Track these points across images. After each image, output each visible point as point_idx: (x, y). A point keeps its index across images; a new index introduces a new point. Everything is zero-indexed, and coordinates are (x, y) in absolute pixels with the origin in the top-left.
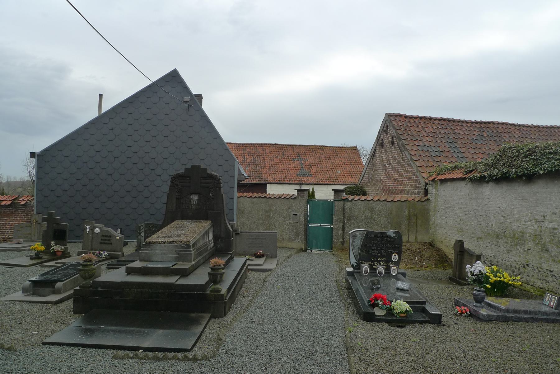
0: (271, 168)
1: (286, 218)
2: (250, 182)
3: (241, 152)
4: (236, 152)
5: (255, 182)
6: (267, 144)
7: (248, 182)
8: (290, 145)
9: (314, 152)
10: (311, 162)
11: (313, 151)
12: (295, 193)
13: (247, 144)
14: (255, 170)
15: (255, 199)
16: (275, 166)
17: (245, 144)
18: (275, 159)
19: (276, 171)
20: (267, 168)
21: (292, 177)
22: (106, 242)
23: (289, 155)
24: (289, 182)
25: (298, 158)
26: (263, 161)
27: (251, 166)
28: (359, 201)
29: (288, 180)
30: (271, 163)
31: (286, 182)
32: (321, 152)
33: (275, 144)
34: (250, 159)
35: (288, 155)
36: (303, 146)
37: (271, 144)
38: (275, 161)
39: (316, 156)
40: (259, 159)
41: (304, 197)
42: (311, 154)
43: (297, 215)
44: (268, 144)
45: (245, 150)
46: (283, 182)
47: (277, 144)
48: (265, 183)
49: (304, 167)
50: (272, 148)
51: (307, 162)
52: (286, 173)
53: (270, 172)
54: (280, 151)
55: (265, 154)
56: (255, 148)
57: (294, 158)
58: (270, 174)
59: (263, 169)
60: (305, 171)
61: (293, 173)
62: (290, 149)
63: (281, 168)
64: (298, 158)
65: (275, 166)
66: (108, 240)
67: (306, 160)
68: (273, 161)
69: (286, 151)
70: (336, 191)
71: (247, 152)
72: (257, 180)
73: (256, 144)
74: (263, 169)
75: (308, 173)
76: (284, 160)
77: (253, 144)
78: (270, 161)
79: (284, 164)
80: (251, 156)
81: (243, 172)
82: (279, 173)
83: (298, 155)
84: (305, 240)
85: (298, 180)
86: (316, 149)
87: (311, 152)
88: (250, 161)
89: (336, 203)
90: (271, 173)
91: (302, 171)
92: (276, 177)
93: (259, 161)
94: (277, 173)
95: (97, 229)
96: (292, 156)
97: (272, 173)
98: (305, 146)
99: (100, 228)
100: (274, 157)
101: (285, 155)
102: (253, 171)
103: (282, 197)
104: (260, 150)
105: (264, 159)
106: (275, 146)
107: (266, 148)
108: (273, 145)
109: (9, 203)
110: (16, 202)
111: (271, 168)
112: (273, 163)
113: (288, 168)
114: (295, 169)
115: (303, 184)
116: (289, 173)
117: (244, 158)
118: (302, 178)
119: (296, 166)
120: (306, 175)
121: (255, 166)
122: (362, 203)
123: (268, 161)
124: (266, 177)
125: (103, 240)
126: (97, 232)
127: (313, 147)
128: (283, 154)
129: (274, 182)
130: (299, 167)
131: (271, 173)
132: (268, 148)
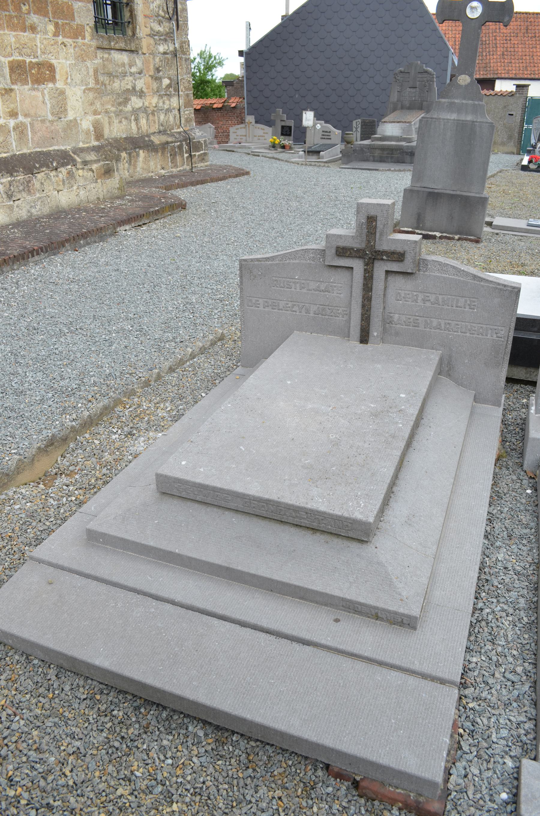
0: (505, 53)
1: (501, 118)
4: (454, 29)
12: (514, 89)
16: (512, 50)
18: (512, 38)
19: (513, 57)
20: (499, 53)
21: (536, 69)
22: (326, 137)
24: (529, 77)
26: (494, 42)
29: (529, 72)
30: (505, 45)
31: (526, 76)
35: (534, 32)
38: (513, 42)
41: (522, 94)
43: (512, 115)
46: (521, 76)
48: (493, 78)
52: (528, 61)
54: (522, 24)
55: (498, 31)
58: (503, 64)
63: (520, 54)
65: (512, 50)
66: (328, 135)
68: (509, 42)
69: (533, 24)
72: (481, 73)
74: (493, 55)
78: (505, 42)
79: (527, 46)
82: (517, 61)
84: (518, 144)
90: (504, 62)
92: (510, 68)
93: (488, 42)
94: (513, 61)
95: (318, 125)
97: (506, 61)
99: (320, 124)
100: (512, 35)
101: (529, 31)
103: (499, 94)
105: (496, 39)
109: (220, 106)
110: (226, 104)
111: (505, 53)
112: (509, 45)
113: (531, 53)
116: (531, 61)
123: (502, 42)
125: (324, 135)
126: (318, 128)
128: (527, 30)
129: (507, 76)
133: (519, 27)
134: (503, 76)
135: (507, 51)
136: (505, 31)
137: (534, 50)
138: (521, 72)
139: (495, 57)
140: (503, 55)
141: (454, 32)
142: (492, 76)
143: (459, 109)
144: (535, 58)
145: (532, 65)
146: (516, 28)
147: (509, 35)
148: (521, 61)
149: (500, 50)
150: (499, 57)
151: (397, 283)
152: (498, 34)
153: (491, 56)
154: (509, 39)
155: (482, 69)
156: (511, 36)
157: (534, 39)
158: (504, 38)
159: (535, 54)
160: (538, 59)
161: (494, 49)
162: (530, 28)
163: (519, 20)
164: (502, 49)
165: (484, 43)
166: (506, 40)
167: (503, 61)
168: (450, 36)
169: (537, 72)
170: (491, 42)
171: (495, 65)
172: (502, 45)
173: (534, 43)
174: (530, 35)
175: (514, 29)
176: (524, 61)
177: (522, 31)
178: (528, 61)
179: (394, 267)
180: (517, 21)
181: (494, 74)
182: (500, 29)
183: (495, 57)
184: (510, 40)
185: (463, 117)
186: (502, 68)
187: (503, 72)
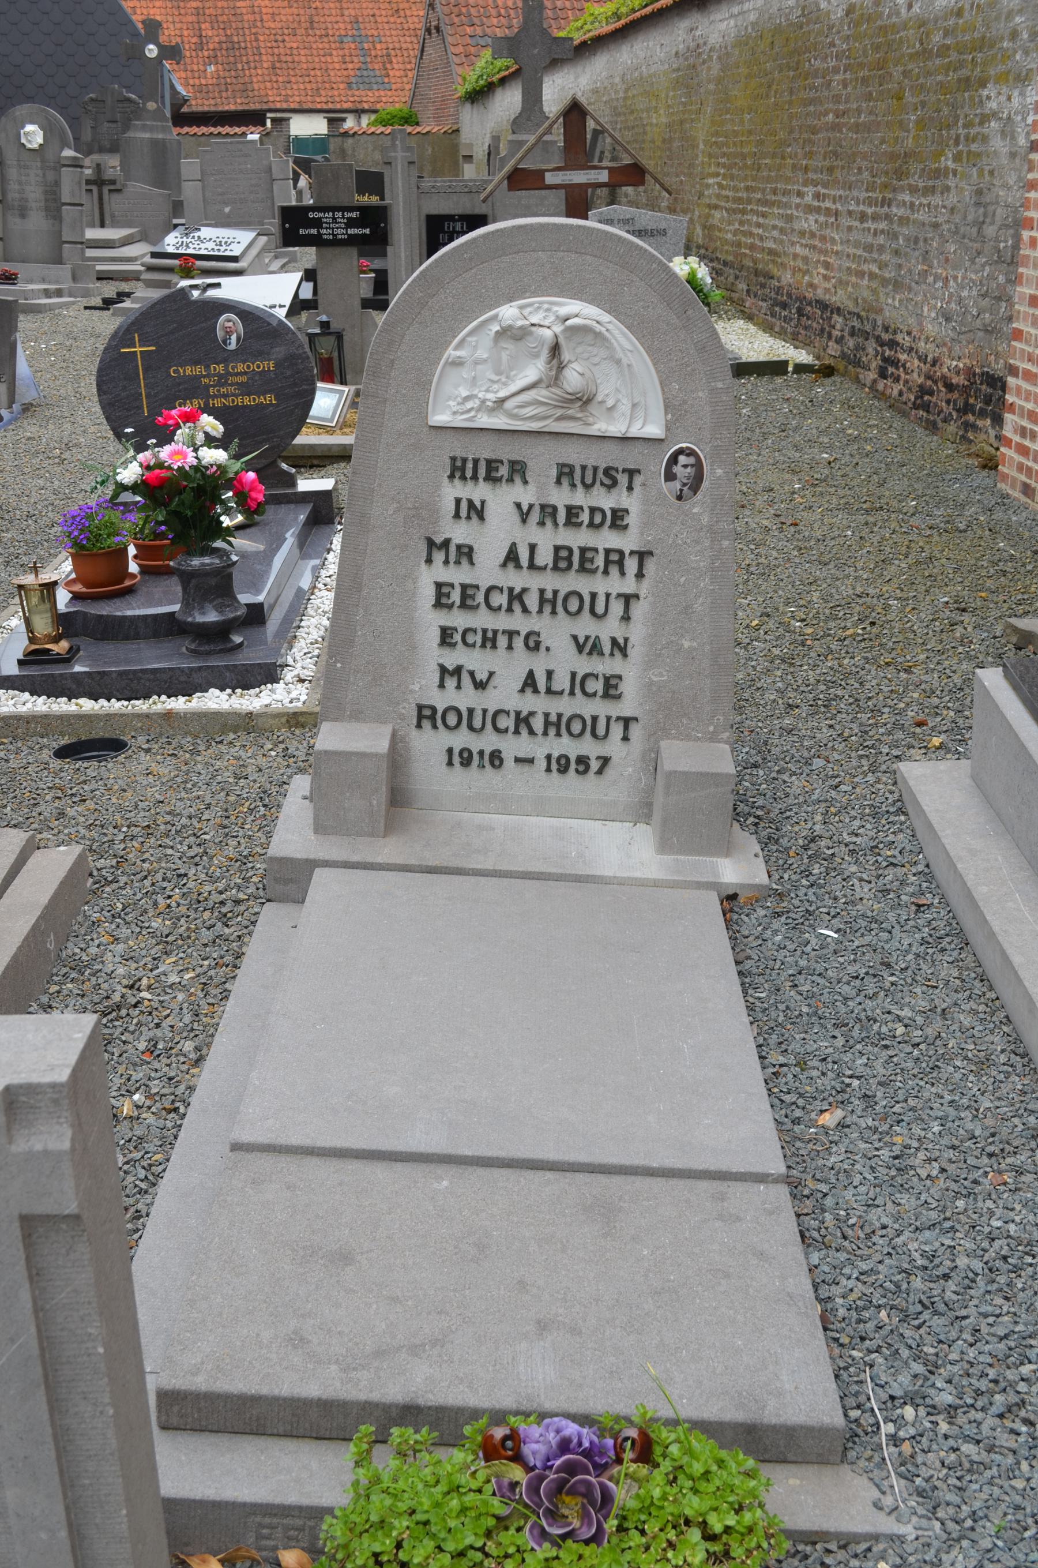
0: (278, 65)
2: (220, 109)
3: (190, 19)
4: (177, 19)
5: (232, 108)
7: (213, 109)
9: (402, 13)
10: (391, 46)
11: (397, 11)
14: (233, 73)
15: (203, 139)
16: (289, 59)
18: (286, 38)
19: (292, 73)
21: (336, 93)
23: (330, 26)
24: (325, 107)
25: (355, 32)
26: (254, 44)
27: (220, 59)
28: (365, 136)
29: (324, 99)
30: (276, 51)
31: (319, 106)
34: (217, 39)
35: (324, 26)
39: (406, 26)
40: (241, 39)
42: (392, 20)
45: (201, 12)
46: (311, 106)
48: (261, 110)
51: (378, 46)
52: (319, 79)
54: (302, 12)
55: (259, 24)
57: (343, 33)
59: (255, 68)
60: (372, 73)
61: (339, 79)
63: (305, 66)
64: (355, 32)
65: (289, 59)
67: (377, 39)
68: (281, 45)
69: (321, 12)
70: (330, 121)
71: (208, 19)
74: (255, 68)
75: (379, 80)
76: (312, 39)
78: (274, 44)
79: (315, 52)
80: (221, 32)
81: (180, 88)
82: (300, 80)
83: (355, 26)
85: (352, 99)
88: (217, 46)
89: (331, 139)
90: (277, 82)
91: (365, 73)
92: (290, 92)
93: (243, 45)
94: (293, 79)
96: (336, 26)
97: (281, 79)
100: (286, 31)
101: (315, 25)
102: (227, 74)
104: (244, 11)
105: (257, 40)
111: (278, 65)
112: (282, 51)
113: (323, 65)
114: (344, 66)
115: (364, 111)
116: (326, 79)
117: (201, 36)
118: (363, 93)
119: (348, 59)
120: (375, 87)
121: (232, 59)
122: (369, 138)
123: (269, 45)
124: (263, 93)
130: (356, 60)
131: (277, 82)
133: (297, 19)
134: (278, 106)
136: (272, 25)
137: (329, 59)
138: (309, 98)
141: (178, 26)
142: (257, 107)
143: (151, 129)
144: (332, 73)
145: (327, 86)
146: (291, 18)
148: (307, 79)
149: (267, 61)
151: (115, 196)
152: (260, 31)
153: (253, 71)
154: (280, 38)
155: (238, 94)
156: (283, 34)
157: (325, 40)
159: (331, 67)
160: (336, 75)
161: (257, 58)
162: (316, 19)
164: (271, 58)
165: (236, 46)
166: (276, 41)
167: (274, 79)
168: (173, 33)
169: (337, 99)
170: (249, 45)
171: (262, 87)
172: (270, 51)
173: (327, 46)
174: (318, 32)
175: (288, 20)
176: (312, 79)
177: (304, 25)
178: (319, 79)
179: (112, 187)
180: (291, 7)
183: (260, 72)
184: (284, 41)
185: (155, 136)
186: (275, 91)
187: (278, 99)
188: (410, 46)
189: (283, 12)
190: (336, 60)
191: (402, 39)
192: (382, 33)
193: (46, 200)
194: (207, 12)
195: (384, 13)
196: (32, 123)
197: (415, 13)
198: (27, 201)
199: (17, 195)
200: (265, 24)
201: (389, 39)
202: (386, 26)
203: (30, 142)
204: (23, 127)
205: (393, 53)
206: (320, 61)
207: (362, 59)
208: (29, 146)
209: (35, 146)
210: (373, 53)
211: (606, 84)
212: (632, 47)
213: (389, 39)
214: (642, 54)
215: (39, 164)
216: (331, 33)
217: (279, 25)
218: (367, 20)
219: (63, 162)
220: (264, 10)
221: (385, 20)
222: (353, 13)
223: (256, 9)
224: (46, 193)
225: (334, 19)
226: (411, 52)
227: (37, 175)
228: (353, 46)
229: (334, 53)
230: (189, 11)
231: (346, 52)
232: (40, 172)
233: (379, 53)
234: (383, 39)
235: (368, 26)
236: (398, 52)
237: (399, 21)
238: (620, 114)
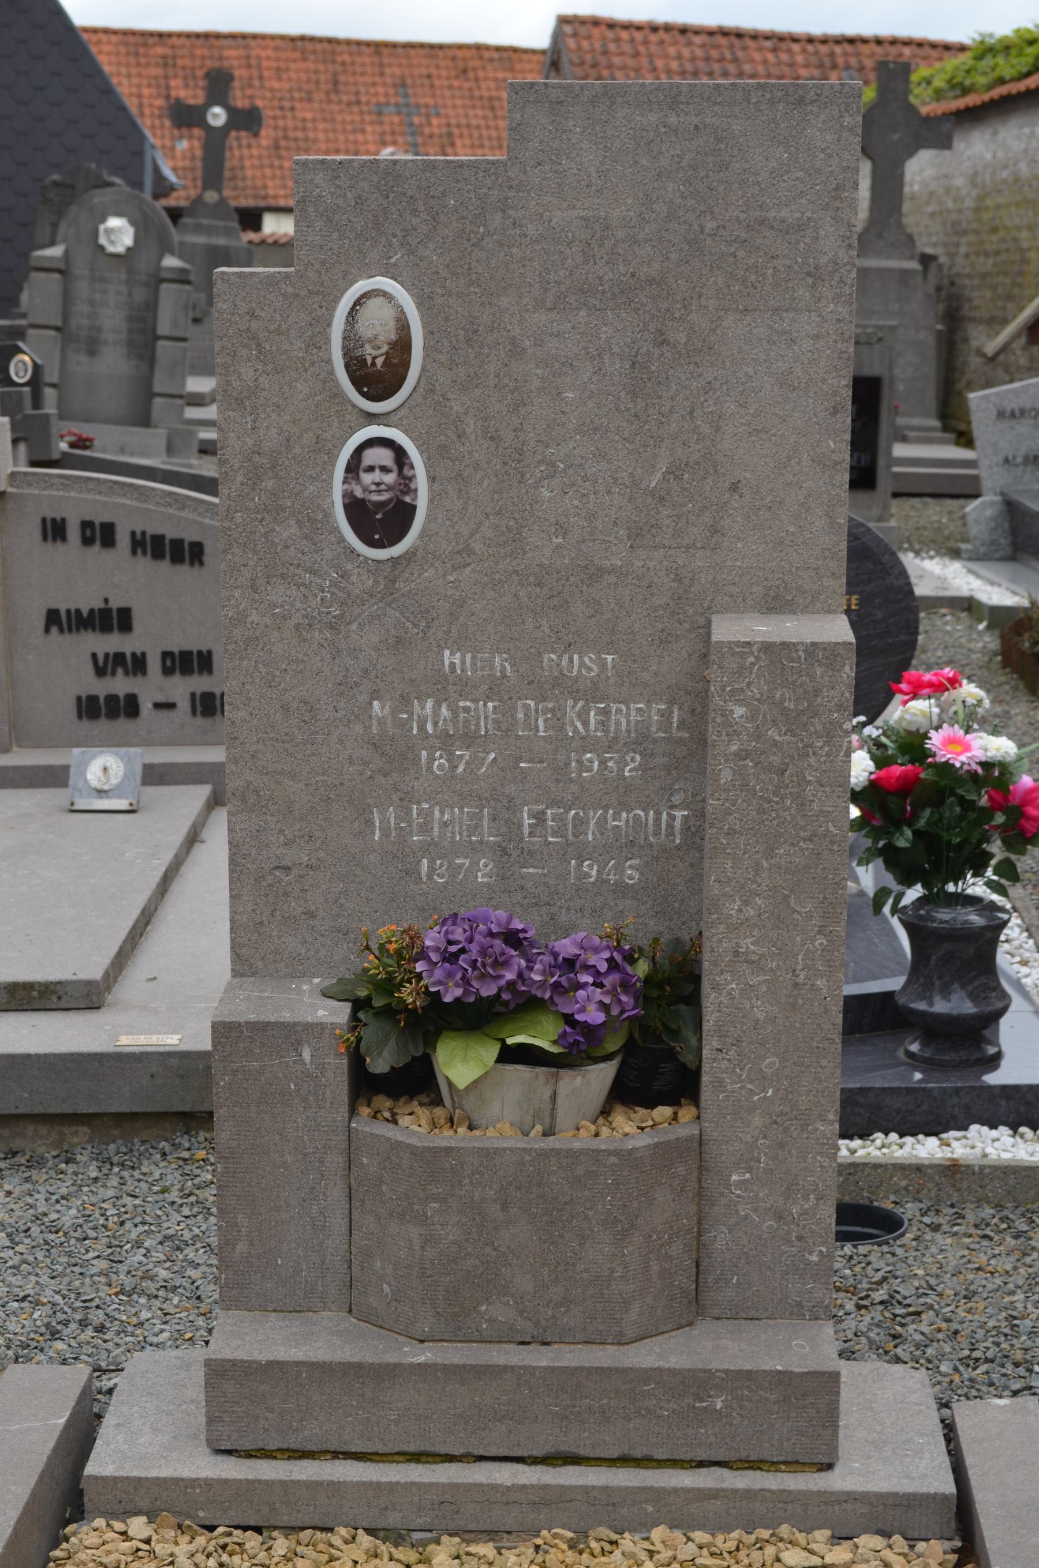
0: (283, 143)
3: (153, 71)
4: (133, 71)
6: (263, 37)
8: (368, 44)
9: (471, 75)
10: (453, 121)
11: (465, 71)
13: (180, 35)
16: (300, 134)
17: (169, 35)
18: (297, 105)
23: (362, 89)
25: (401, 100)
30: (281, 123)
32: (500, 75)
33: (303, 38)
35: (353, 89)
36: (422, 46)
37: (283, 38)
39: (477, 94)
42: (456, 83)
44: (273, 37)
45: (170, 62)
47: (312, 39)
49: (419, 140)
50: (289, 54)
51: (435, 121)
53: (276, 163)
54: (321, 67)
55: (256, 83)
56: (216, 53)
57: (382, 100)
59: (249, 146)
62: (367, 60)
64: (401, 100)
65: (300, 134)
67: (433, 111)
68: (289, 114)
71: (180, 73)
73: (218, 36)
76: (335, 107)
77: (207, 36)
78: (278, 113)
79: (339, 127)
83: (401, 91)
86: (477, 63)
87: (457, 77)
96: (372, 90)
98: (432, 47)
100: (297, 95)
101: (341, 88)
104: (235, 63)
106: (299, 44)
107: (263, 54)
108: (293, 39)
112: (290, 123)
124: (259, 183)
127: (468, 53)
128: (336, 83)
132: (270, 52)
133: (314, 77)
135: (286, 138)
136: (276, 85)
137: (360, 137)
139: (255, 152)
140: (277, 147)
141: (135, 81)
143: (209, 231)
146: (304, 76)
147: (287, 95)
150: (265, 153)
153: (245, 152)
154: (287, 104)
157: (356, 109)
158: (276, 103)
162: (342, 78)
163: (312, 57)
164: (272, 133)
166: (282, 108)
167: (276, 163)
173: (357, 118)
174: (345, 98)
175: (299, 80)
177: (323, 87)
181: (256, 197)
182: (261, 78)
186: (278, 182)
187: (282, 192)
188: (482, 122)
189: (293, 66)
190: (370, 138)
191: (471, 113)
192: (440, 102)
193: (131, 331)
194: (180, 62)
195: (444, 73)
196: (118, 214)
197: (491, 75)
198: (99, 330)
199: (85, 322)
200: (267, 84)
201: (451, 112)
202: (448, 93)
203: (112, 243)
204: (103, 220)
205: (456, 131)
206: (347, 141)
207: (410, 139)
208: (111, 249)
209: (120, 249)
210: (427, 131)
211: (933, 186)
212: (995, 133)
213: (451, 112)
214: (1018, 146)
215: (123, 277)
216: (364, 99)
217: (287, 86)
218: (419, 82)
219: (164, 275)
220: (265, 64)
221: (446, 83)
222: (398, 71)
223: (253, 62)
224: (130, 319)
225: (367, 79)
226: (485, 133)
227: (119, 293)
228: (396, 119)
229: (369, 128)
230: (153, 61)
231: (387, 128)
232: (124, 289)
233: (436, 131)
234: (443, 112)
235: (420, 91)
236: (465, 132)
237: (466, 85)
238: (965, 232)
